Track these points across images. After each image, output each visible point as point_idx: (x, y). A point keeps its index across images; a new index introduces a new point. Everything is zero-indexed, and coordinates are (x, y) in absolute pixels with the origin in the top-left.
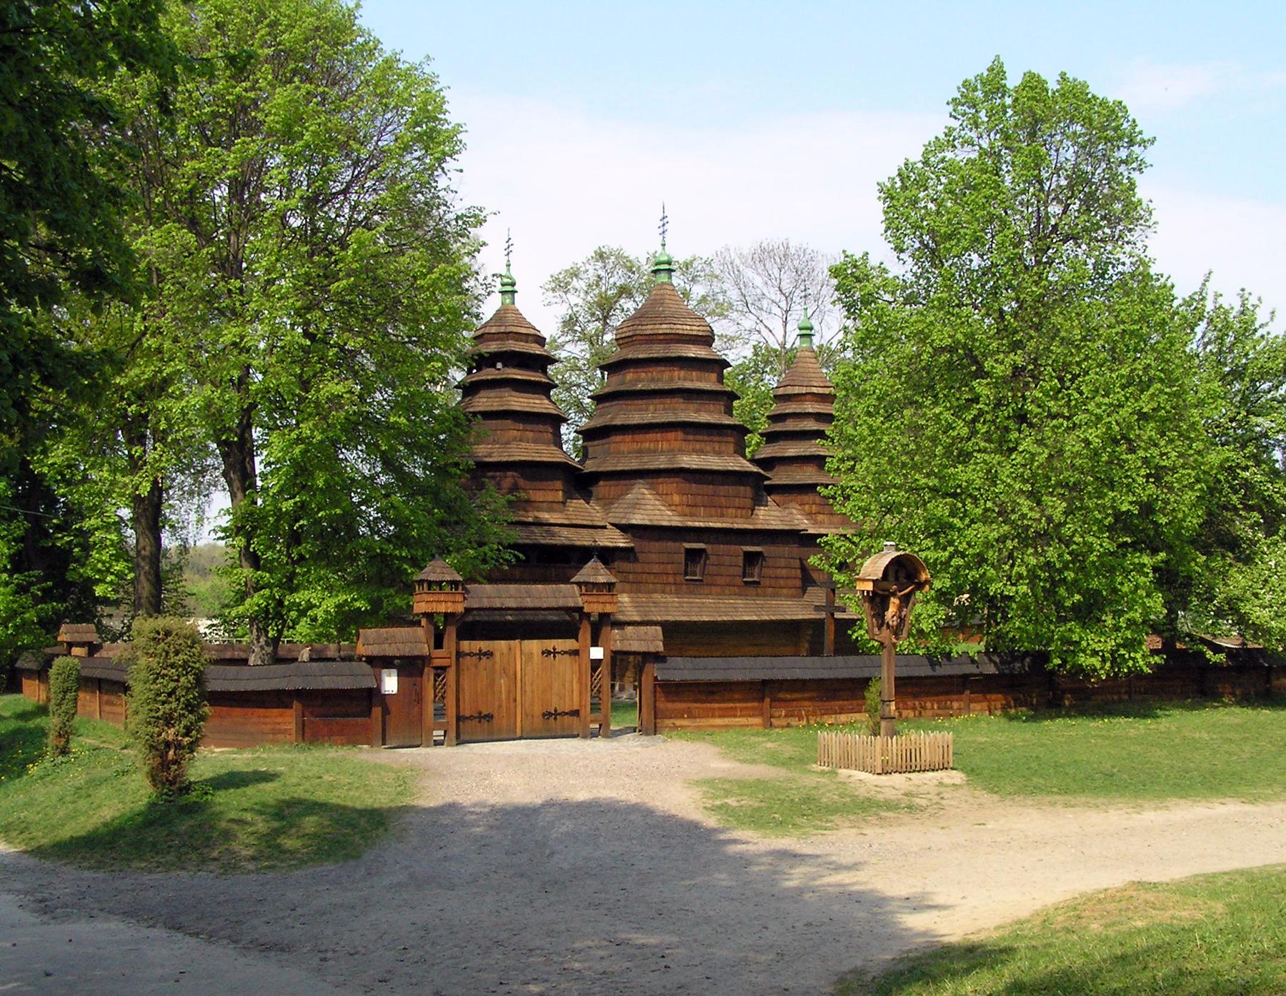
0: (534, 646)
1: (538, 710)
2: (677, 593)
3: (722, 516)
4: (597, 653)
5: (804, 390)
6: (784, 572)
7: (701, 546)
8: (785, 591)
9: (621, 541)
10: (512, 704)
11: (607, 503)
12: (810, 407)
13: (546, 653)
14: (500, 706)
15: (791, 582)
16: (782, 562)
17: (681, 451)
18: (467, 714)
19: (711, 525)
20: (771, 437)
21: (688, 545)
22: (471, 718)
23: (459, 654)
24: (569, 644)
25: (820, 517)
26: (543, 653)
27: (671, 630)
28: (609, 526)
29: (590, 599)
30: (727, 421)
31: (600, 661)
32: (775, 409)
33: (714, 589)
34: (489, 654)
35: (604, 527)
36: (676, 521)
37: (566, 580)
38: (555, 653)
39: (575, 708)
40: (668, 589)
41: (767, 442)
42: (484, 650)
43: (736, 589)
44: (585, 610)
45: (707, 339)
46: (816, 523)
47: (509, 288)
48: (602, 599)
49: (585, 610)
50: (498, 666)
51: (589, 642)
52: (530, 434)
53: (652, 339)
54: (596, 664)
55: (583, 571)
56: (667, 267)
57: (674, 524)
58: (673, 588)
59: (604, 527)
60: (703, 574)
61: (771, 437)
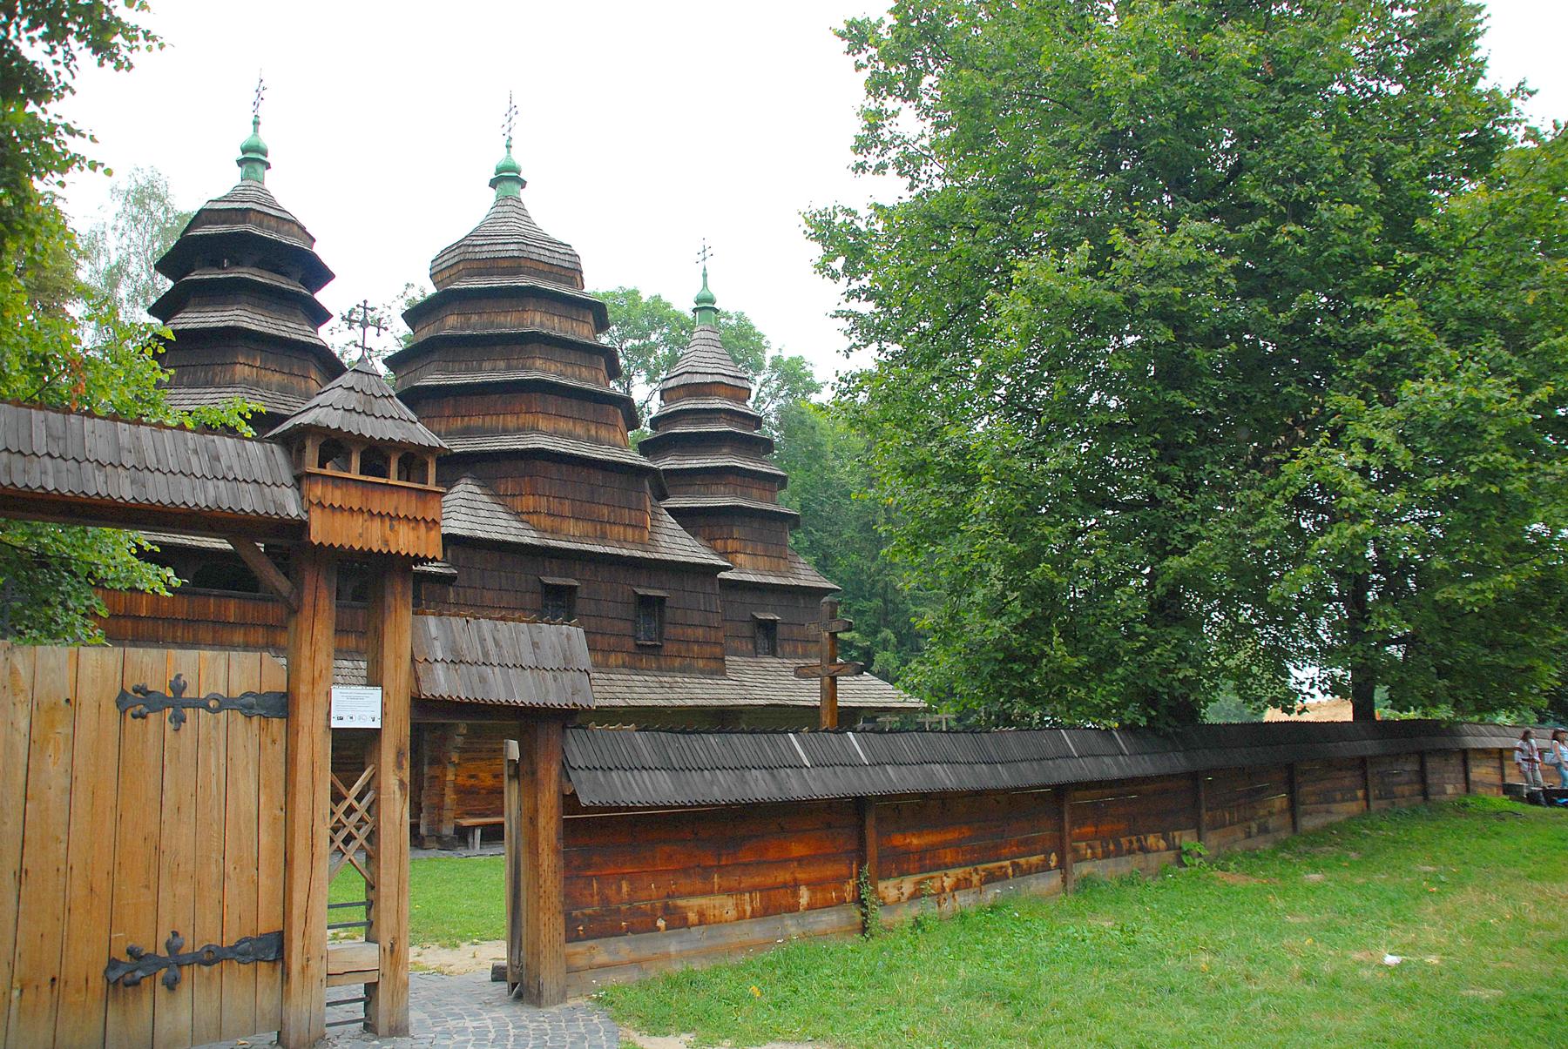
4: (357, 706)
5: (709, 379)
6: (700, 631)
8: (701, 663)
13: (136, 702)
15: (708, 650)
16: (696, 618)
17: (535, 429)
21: (548, 580)
26: (122, 700)
29: (336, 497)
31: (374, 734)
36: (530, 538)
38: (176, 702)
39: (268, 923)
44: (316, 536)
48: (388, 503)
49: (316, 536)
54: (352, 749)
57: (528, 540)
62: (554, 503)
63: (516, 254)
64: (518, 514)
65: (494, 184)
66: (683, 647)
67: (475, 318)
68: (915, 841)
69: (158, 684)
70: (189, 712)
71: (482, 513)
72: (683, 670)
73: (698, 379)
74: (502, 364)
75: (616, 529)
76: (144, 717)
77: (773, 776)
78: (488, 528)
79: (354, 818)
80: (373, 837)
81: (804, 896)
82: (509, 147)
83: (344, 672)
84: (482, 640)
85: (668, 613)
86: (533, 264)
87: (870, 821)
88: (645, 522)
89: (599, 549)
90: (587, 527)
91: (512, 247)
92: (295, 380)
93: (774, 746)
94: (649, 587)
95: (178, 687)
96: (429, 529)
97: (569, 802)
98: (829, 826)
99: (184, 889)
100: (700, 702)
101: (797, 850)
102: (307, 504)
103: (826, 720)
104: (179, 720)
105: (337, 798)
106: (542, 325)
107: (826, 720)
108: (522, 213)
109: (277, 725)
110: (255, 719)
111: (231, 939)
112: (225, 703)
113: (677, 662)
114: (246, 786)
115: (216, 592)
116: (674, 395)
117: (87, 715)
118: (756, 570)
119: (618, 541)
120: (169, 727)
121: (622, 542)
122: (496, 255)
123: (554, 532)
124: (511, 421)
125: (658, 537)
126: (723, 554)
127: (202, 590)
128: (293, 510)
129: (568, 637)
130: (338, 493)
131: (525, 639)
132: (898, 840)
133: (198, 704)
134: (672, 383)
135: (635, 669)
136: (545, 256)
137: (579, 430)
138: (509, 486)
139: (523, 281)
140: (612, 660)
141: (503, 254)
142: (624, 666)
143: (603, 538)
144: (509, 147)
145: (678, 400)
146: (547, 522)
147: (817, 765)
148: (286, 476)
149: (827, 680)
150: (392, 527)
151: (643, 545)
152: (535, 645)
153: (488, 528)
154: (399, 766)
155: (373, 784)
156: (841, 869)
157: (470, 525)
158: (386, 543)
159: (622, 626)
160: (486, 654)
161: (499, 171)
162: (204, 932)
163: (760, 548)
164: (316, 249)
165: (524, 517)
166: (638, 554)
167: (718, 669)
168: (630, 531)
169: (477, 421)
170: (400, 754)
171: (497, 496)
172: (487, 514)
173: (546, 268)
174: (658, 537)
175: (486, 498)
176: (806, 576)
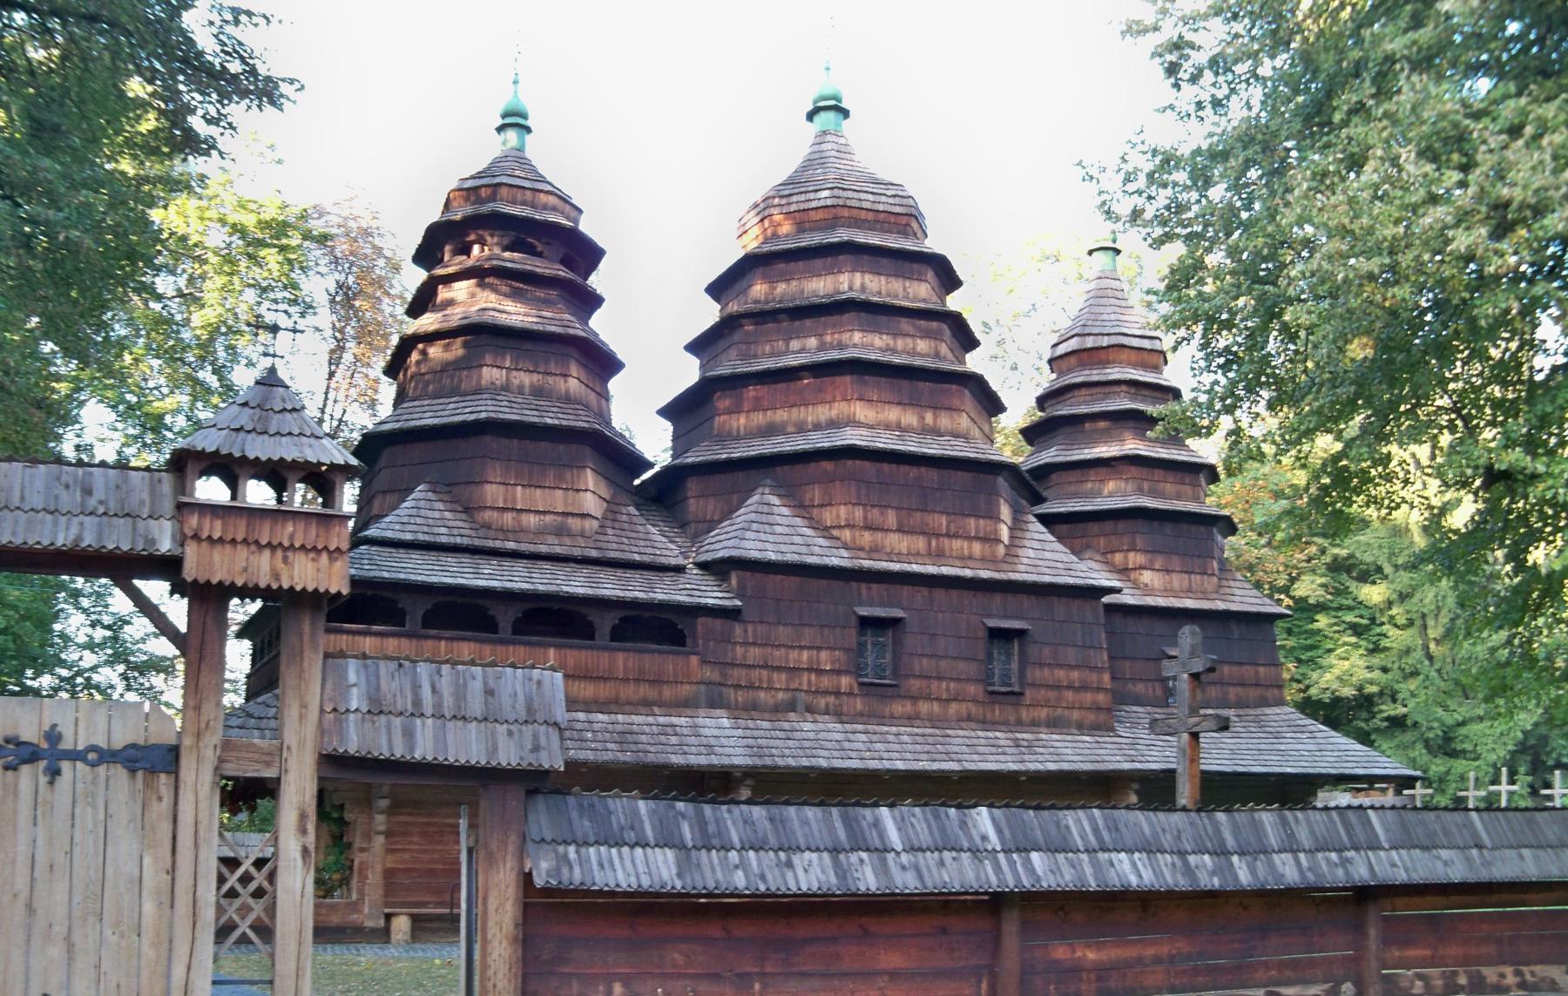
2: (839, 715)
5: (1105, 342)
6: (1075, 675)
7: (897, 613)
8: (1076, 715)
9: (713, 596)
12: (1114, 373)
15: (1088, 697)
16: (1071, 655)
17: (852, 422)
19: (915, 568)
25: (1147, 577)
33: (924, 707)
35: (679, 569)
36: (839, 559)
40: (821, 702)
43: (973, 708)
45: (907, 219)
46: (1136, 585)
52: (525, 379)
53: (802, 221)
57: (835, 561)
58: (831, 699)
60: (896, 673)
62: (875, 514)
63: (829, 202)
64: (827, 529)
65: (811, 116)
66: (1051, 694)
67: (781, 288)
68: (1091, 955)
69: (30, 733)
70: (66, 766)
71: (779, 529)
72: (1054, 724)
73: (1090, 342)
74: (812, 342)
75: (957, 544)
76: (15, 769)
77: (836, 864)
78: (783, 548)
79: (253, 886)
80: (271, 910)
83: (596, 727)
84: (416, 687)
85: (1033, 651)
86: (846, 213)
88: (996, 531)
89: (931, 570)
90: (920, 543)
91: (826, 193)
92: (550, 380)
93: (848, 822)
94: (1006, 617)
95: (53, 736)
96: (332, 560)
97: (527, 879)
98: (944, 931)
99: (56, 951)
100: (1066, 766)
101: (892, 959)
103: (1185, 793)
104: (54, 773)
106: (863, 288)
107: (1185, 793)
108: (844, 151)
110: (140, 774)
112: (106, 756)
113: (1043, 713)
114: (124, 848)
115: (447, 634)
116: (1064, 364)
118: (1168, 591)
119: (962, 558)
120: (43, 780)
121: (966, 559)
122: (806, 206)
123: (874, 551)
124: (823, 413)
125: (1020, 552)
126: (1123, 571)
127: (433, 632)
128: (165, 546)
129: (539, 683)
130: (218, 524)
131: (476, 686)
132: (1060, 952)
133: (75, 756)
134: (1061, 350)
135: (986, 724)
136: (867, 201)
137: (910, 418)
138: (816, 494)
139: (842, 235)
140: (954, 708)
141: (814, 204)
142: (969, 719)
143: (939, 556)
145: (1070, 370)
146: (867, 538)
147: (912, 849)
148: (168, 506)
149: (1185, 736)
150: (285, 560)
151: (992, 561)
152: (489, 692)
153: (783, 548)
154: (303, 831)
157: (760, 545)
158: (277, 576)
159: (971, 669)
160: (417, 702)
163: (1176, 562)
164: (585, 227)
165: (835, 533)
166: (985, 574)
167: (1102, 726)
168: (977, 548)
169: (781, 415)
170: (303, 816)
171: (801, 507)
172: (787, 530)
173: (870, 216)
174: (1020, 552)
175: (785, 511)
176: (1243, 599)
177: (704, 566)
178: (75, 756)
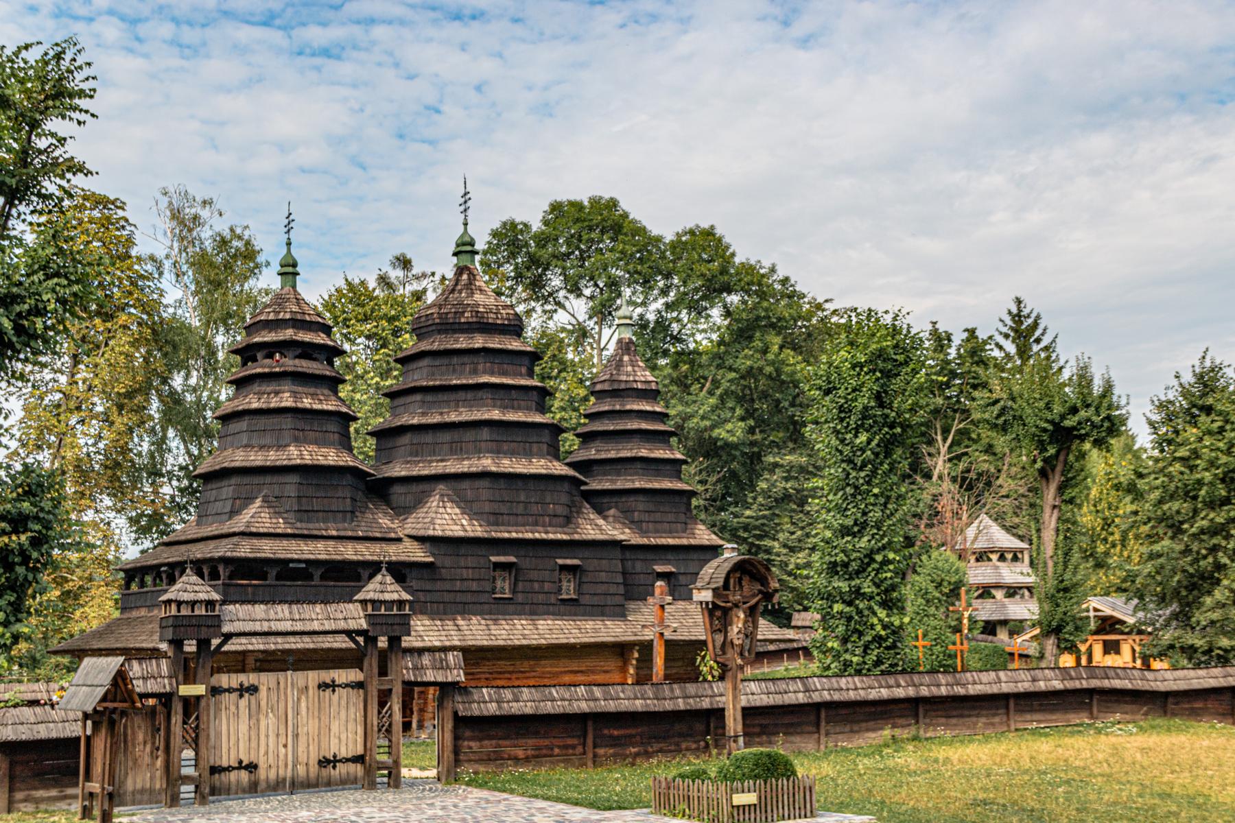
0: (313, 677)
1: (313, 762)
3: (536, 524)
7: (512, 559)
9: (418, 554)
10: (282, 750)
11: (402, 511)
13: (323, 686)
14: (267, 753)
18: (225, 764)
20: (587, 438)
22: (229, 769)
23: (215, 691)
24: (354, 675)
26: (319, 687)
27: (474, 656)
28: (406, 539)
30: (538, 418)
32: (592, 405)
34: (253, 689)
35: (399, 540)
37: (351, 601)
41: (583, 443)
42: (246, 684)
47: (290, 269)
50: (263, 703)
51: (376, 670)
55: (370, 586)
56: (469, 248)
59: (399, 540)
61: (587, 438)
65: (455, 254)
68: (616, 733)
69: (328, 681)
80: (390, 725)
81: (557, 751)
82: (466, 224)
87: (590, 723)
95: (333, 681)
97: (456, 713)
102: (369, 624)
104: (334, 691)
105: (379, 713)
109: (361, 691)
111: (350, 756)
112: (347, 685)
117: (311, 692)
128: (365, 626)
132: (606, 732)
133: (339, 686)
144: (466, 224)
155: (390, 708)
156: (575, 741)
161: (458, 245)
162: (343, 753)
177: (410, 536)
178: (339, 686)
